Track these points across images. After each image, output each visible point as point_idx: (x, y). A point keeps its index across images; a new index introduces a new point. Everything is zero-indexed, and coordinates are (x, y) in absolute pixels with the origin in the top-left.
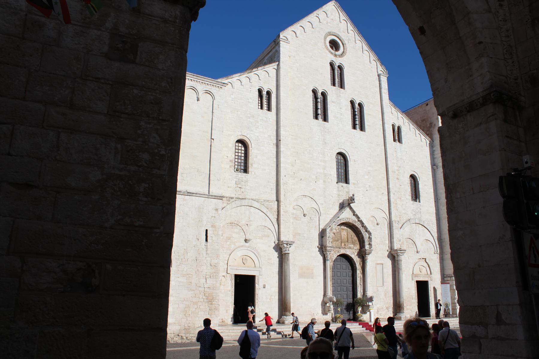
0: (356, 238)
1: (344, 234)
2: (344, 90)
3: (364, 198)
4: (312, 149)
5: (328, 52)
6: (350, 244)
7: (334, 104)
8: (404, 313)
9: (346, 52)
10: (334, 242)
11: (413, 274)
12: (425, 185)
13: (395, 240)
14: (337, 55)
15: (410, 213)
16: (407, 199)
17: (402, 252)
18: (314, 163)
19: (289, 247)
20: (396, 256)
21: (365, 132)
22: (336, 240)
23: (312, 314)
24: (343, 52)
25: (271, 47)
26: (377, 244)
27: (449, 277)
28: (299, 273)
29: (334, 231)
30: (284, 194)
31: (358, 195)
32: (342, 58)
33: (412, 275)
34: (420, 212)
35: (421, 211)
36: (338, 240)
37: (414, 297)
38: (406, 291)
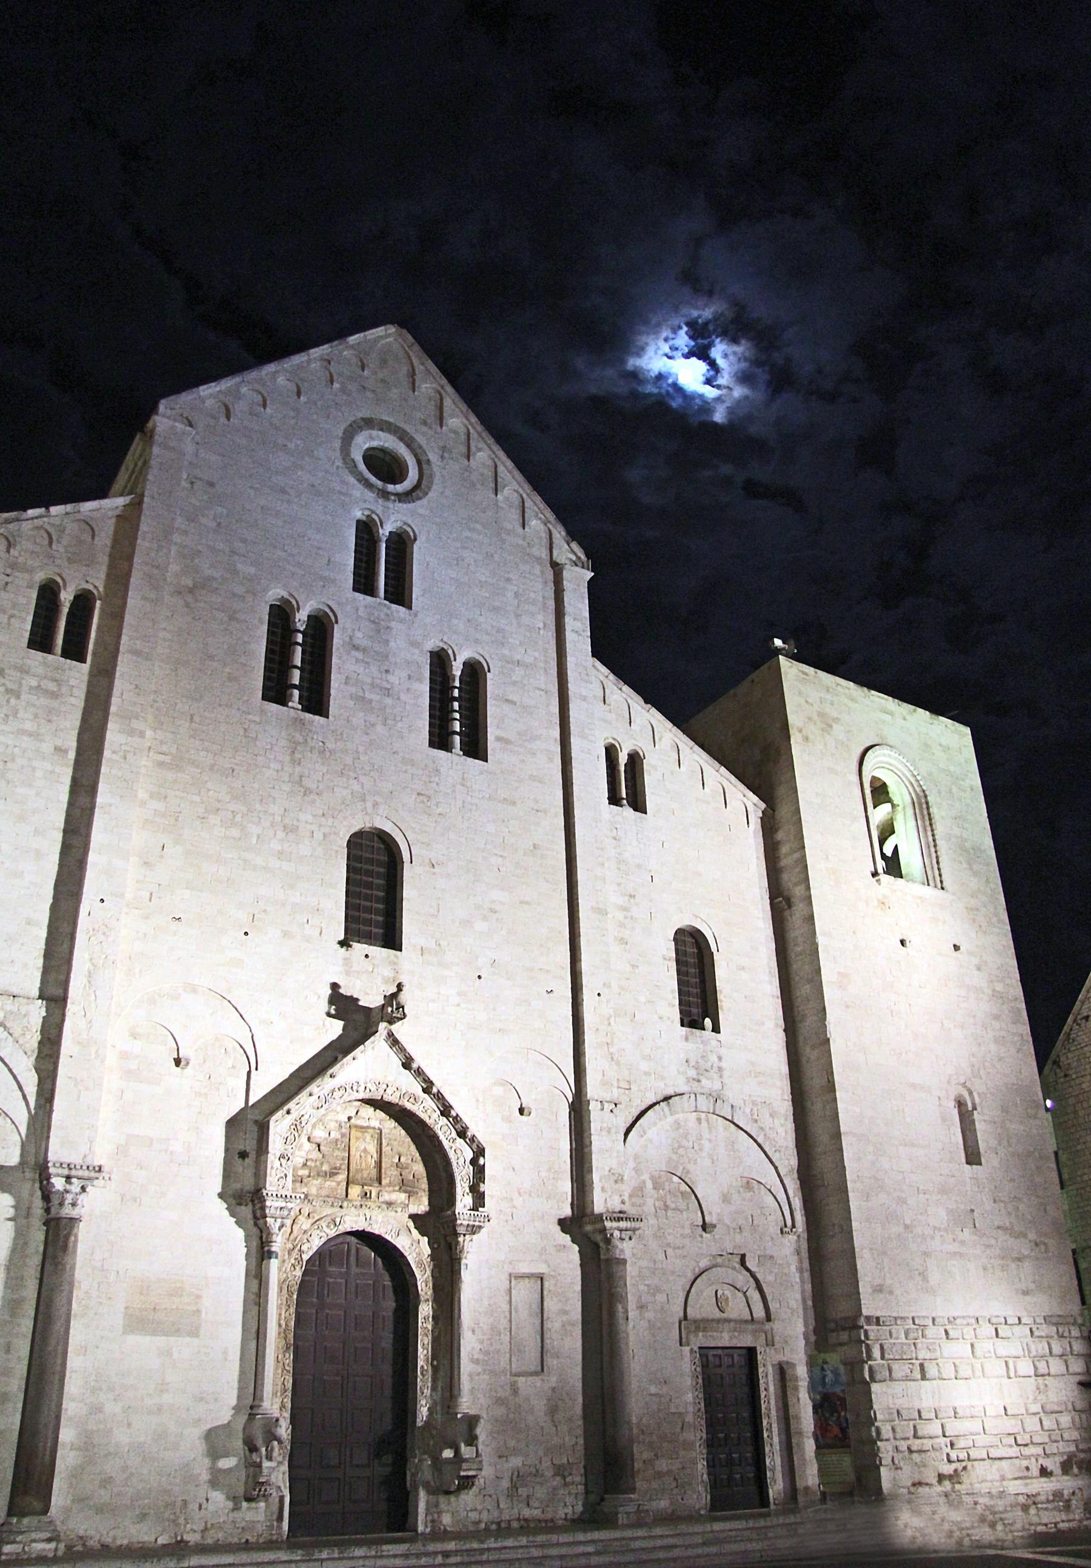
0: (419, 1168)
1: (365, 1151)
2: (407, 611)
3: (463, 1005)
4: (244, 809)
5: (352, 480)
6: (390, 1192)
7: (359, 655)
8: (633, 1490)
9: (429, 488)
10: (315, 1182)
11: (685, 1317)
12: (743, 968)
13: (596, 1177)
14: (388, 493)
15: (676, 1073)
16: (660, 1018)
17: (623, 1224)
18: (245, 861)
19: (78, 1190)
20: (598, 1238)
21: (485, 759)
22: (326, 1173)
23: (179, 1504)
24: (417, 487)
25: (134, 455)
26: (520, 1194)
27: (844, 1329)
28: (126, 1308)
29: (319, 1134)
30: (89, 972)
31: (439, 993)
32: (411, 506)
33: (680, 1323)
34: (720, 1069)
35: (724, 1064)
36: (332, 1174)
37: (689, 1418)
38: (653, 1392)
